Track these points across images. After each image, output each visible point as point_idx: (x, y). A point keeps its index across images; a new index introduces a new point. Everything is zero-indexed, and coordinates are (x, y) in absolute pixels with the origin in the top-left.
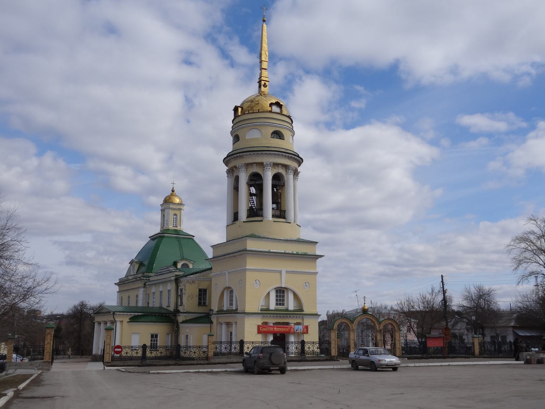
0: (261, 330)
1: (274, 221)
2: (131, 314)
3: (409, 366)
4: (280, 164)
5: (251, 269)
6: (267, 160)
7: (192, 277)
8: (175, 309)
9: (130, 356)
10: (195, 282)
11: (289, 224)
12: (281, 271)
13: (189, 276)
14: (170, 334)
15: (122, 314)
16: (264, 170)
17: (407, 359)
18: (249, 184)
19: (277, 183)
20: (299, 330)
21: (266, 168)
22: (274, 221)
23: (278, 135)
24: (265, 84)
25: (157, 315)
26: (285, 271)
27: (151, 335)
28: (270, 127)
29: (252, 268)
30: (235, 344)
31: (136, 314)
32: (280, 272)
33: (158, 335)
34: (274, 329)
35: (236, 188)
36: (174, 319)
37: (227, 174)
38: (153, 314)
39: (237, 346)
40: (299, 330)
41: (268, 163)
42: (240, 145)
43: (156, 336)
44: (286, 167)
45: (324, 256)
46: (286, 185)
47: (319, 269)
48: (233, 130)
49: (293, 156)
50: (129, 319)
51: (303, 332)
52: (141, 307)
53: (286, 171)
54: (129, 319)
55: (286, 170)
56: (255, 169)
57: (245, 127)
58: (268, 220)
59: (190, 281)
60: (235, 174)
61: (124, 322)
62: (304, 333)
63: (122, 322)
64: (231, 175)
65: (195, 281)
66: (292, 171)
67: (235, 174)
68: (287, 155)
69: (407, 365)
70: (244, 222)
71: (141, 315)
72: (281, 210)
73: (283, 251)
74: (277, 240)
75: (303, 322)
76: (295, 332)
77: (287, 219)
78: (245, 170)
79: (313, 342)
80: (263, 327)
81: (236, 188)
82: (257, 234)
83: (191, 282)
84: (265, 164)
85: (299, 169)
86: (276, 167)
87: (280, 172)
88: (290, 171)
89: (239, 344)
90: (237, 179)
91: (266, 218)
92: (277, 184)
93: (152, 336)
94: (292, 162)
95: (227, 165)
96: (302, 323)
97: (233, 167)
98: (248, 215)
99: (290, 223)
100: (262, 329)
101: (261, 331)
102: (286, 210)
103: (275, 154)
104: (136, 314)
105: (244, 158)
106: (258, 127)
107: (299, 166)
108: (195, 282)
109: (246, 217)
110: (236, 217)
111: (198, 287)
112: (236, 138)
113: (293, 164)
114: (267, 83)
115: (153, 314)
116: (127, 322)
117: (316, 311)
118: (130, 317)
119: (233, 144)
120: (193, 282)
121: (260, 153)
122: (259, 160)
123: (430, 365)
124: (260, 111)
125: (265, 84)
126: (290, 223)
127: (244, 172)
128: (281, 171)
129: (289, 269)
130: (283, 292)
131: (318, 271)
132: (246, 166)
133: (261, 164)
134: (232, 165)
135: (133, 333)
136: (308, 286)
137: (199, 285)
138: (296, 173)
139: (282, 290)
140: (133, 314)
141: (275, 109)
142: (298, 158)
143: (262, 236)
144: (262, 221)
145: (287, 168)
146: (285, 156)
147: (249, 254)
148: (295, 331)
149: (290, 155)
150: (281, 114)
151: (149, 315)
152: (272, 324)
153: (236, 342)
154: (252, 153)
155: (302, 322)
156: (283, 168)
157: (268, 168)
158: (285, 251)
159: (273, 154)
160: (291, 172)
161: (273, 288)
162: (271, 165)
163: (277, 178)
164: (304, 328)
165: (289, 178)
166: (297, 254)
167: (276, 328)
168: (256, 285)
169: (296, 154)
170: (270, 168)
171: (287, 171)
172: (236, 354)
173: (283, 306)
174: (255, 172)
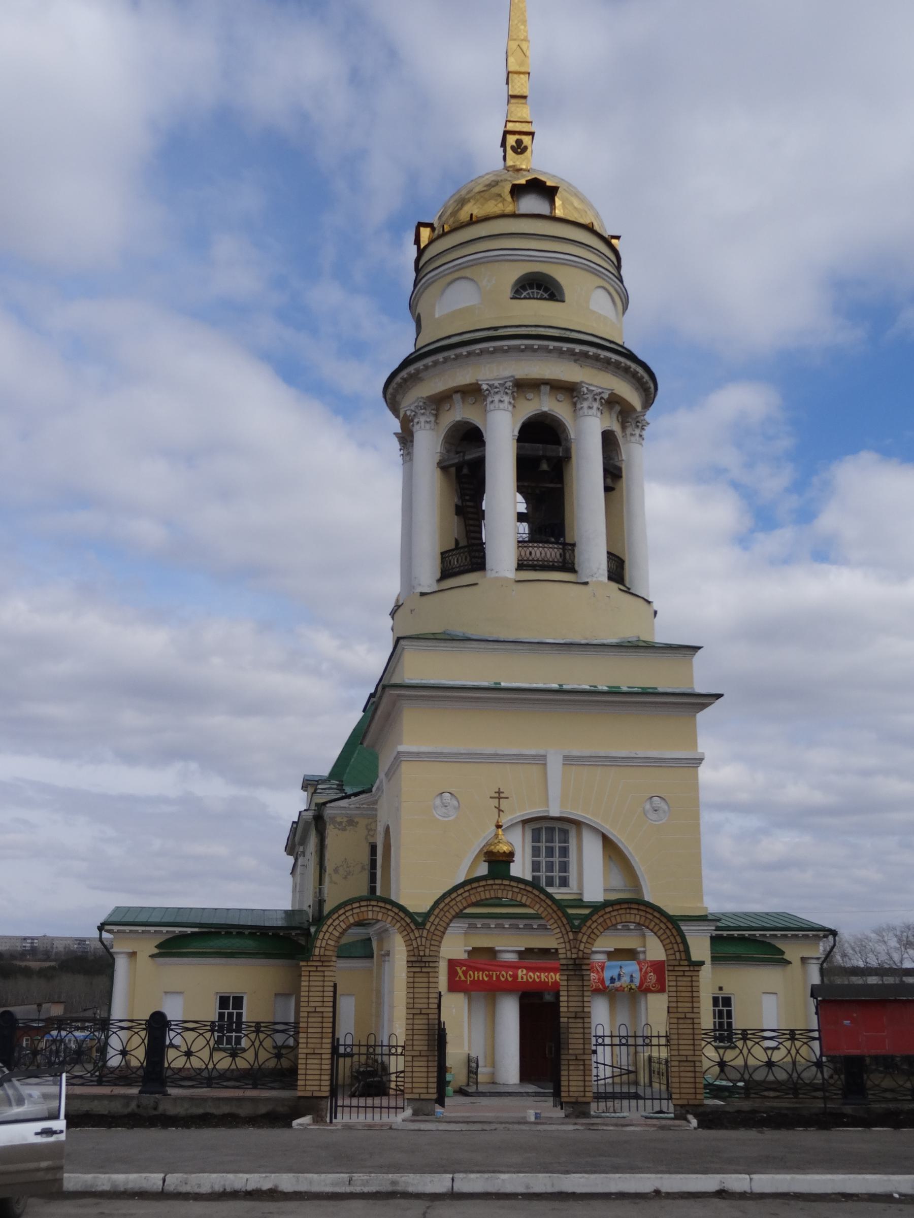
0: (463, 978)
2: (161, 932)
3: (411, 1189)
5: (418, 754)
7: (347, 805)
8: (317, 914)
9: (248, 1066)
10: (357, 823)
11: (582, 587)
12: (544, 757)
13: (332, 804)
14: (294, 996)
15: (131, 931)
17: (694, 1122)
18: (447, 463)
20: (625, 980)
21: (489, 399)
24: (519, 142)
25: (247, 932)
26: (562, 757)
27: (221, 998)
28: (507, 264)
29: (424, 749)
30: (124, 1034)
31: (177, 930)
32: (541, 760)
33: (242, 998)
34: (515, 976)
36: (303, 943)
38: (234, 931)
39: (136, 1040)
40: (625, 980)
41: (496, 383)
43: (238, 1002)
44: (570, 391)
45: (719, 696)
47: (706, 745)
49: (592, 351)
50: (156, 947)
51: (642, 983)
52: (290, 910)
53: (575, 404)
54: (156, 947)
55: (575, 404)
56: (459, 412)
57: (433, 282)
58: (497, 578)
59: (339, 819)
61: (139, 956)
62: (648, 991)
63: (133, 955)
65: (356, 820)
66: (596, 405)
68: (565, 346)
69: (394, 1183)
71: (193, 934)
72: (565, 544)
73: (555, 686)
74: (526, 647)
75: (644, 947)
76: (606, 988)
77: (580, 572)
78: (432, 419)
79: (258, 1023)
80: (470, 968)
82: (459, 630)
83: (344, 825)
84: (485, 387)
86: (530, 396)
87: (545, 409)
88: (585, 404)
89: (143, 1033)
91: (492, 570)
92: (541, 453)
93: (224, 1002)
94: (594, 372)
96: (639, 953)
98: (442, 572)
99: (586, 583)
100: (465, 973)
101: (460, 981)
102: (576, 539)
103: (517, 349)
104: (177, 930)
105: (421, 380)
106: (467, 273)
108: (357, 823)
111: (366, 839)
114: (526, 140)
115: (234, 931)
116: (150, 956)
117: (699, 905)
118: (162, 940)
120: (351, 822)
121: (464, 351)
122: (463, 376)
123: (570, 1190)
124: (474, 219)
125: (519, 142)
126: (586, 583)
127: (428, 426)
128: (557, 407)
129: (575, 752)
130: (565, 833)
131: (703, 753)
132: (434, 407)
135: (166, 993)
136: (664, 812)
137: (371, 833)
139: (559, 828)
140: (165, 929)
141: (532, 204)
142: (629, 363)
143: (471, 632)
145: (575, 394)
146: (560, 352)
147: (410, 698)
148: (607, 983)
149: (578, 348)
151: (220, 933)
152: (511, 957)
153: (131, 1025)
154: (440, 357)
155: (642, 949)
156: (560, 397)
157: (496, 398)
158: (561, 685)
159: (510, 349)
160: (590, 408)
161: (511, 820)
162: (506, 388)
164: (646, 973)
166: (614, 692)
167: (525, 971)
168: (444, 810)
169: (620, 349)
170: (506, 399)
171: (579, 406)
172: (123, 1076)
173: (564, 890)
174: (458, 422)
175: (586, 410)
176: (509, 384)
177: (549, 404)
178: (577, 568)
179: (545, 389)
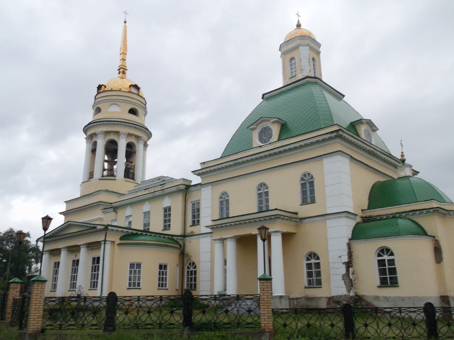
1: (126, 181)
4: (134, 135)
6: (124, 130)
16: (119, 138)
19: (130, 150)
21: (121, 136)
22: (126, 181)
23: (133, 111)
35: (94, 151)
37: (87, 140)
42: (100, 116)
44: (138, 137)
46: (137, 152)
48: (94, 103)
56: (112, 137)
60: (94, 140)
64: (90, 141)
66: (143, 142)
67: (94, 140)
70: (99, 179)
78: (104, 136)
81: (94, 151)
84: (121, 133)
85: (148, 143)
87: (133, 141)
88: (141, 142)
90: (95, 144)
95: (86, 134)
97: (92, 133)
107: (148, 140)
109: (101, 176)
110: (91, 175)
112: (98, 110)
113: (145, 137)
119: (94, 115)
133: (117, 133)
134: (89, 133)
138: (146, 145)
144: (115, 180)
145: (139, 138)
150: (138, 95)
156: (136, 139)
163: (130, 147)
165: (139, 147)
171: (139, 142)
175: (141, 143)
176: (127, 133)
177: (133, 140)
178: (135, 179)
179: (133, 136)
